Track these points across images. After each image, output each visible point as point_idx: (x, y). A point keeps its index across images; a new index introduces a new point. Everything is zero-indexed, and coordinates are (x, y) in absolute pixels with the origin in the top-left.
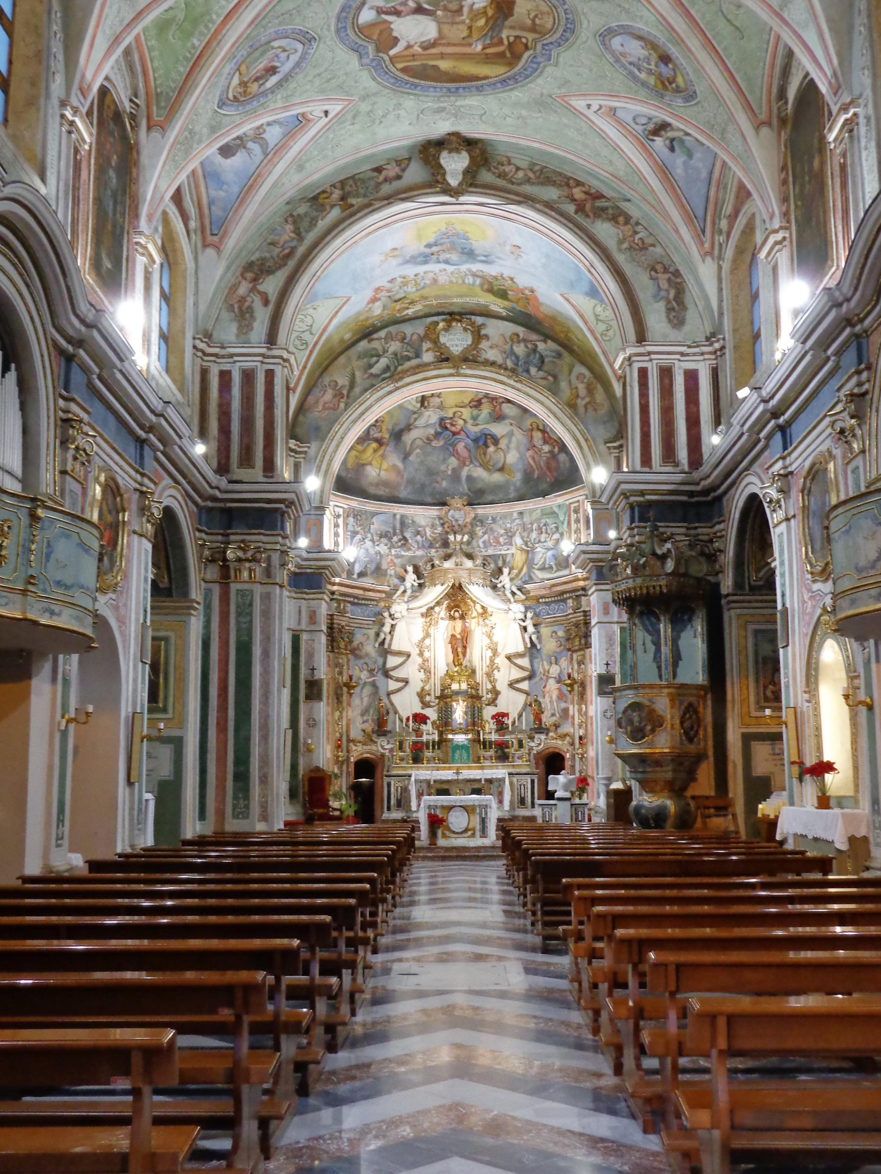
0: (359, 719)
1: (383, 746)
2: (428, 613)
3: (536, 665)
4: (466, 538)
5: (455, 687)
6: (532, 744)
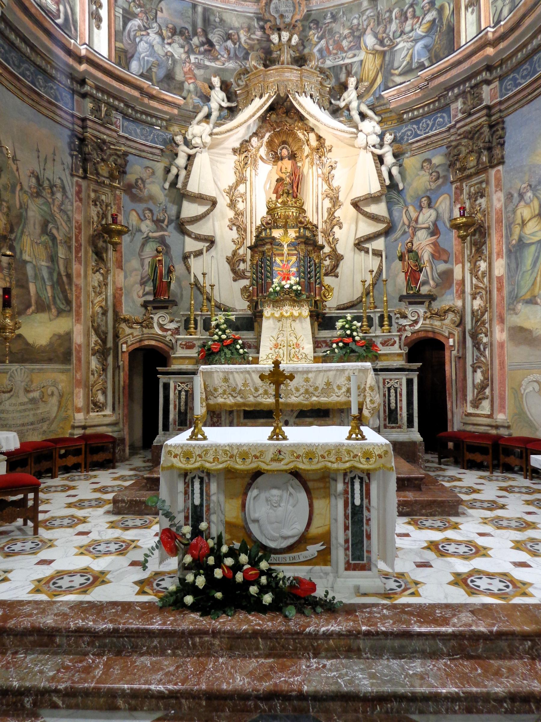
1: (163, 325)
2: (243, 148)
3: (396, 214)
4: (295, 39)
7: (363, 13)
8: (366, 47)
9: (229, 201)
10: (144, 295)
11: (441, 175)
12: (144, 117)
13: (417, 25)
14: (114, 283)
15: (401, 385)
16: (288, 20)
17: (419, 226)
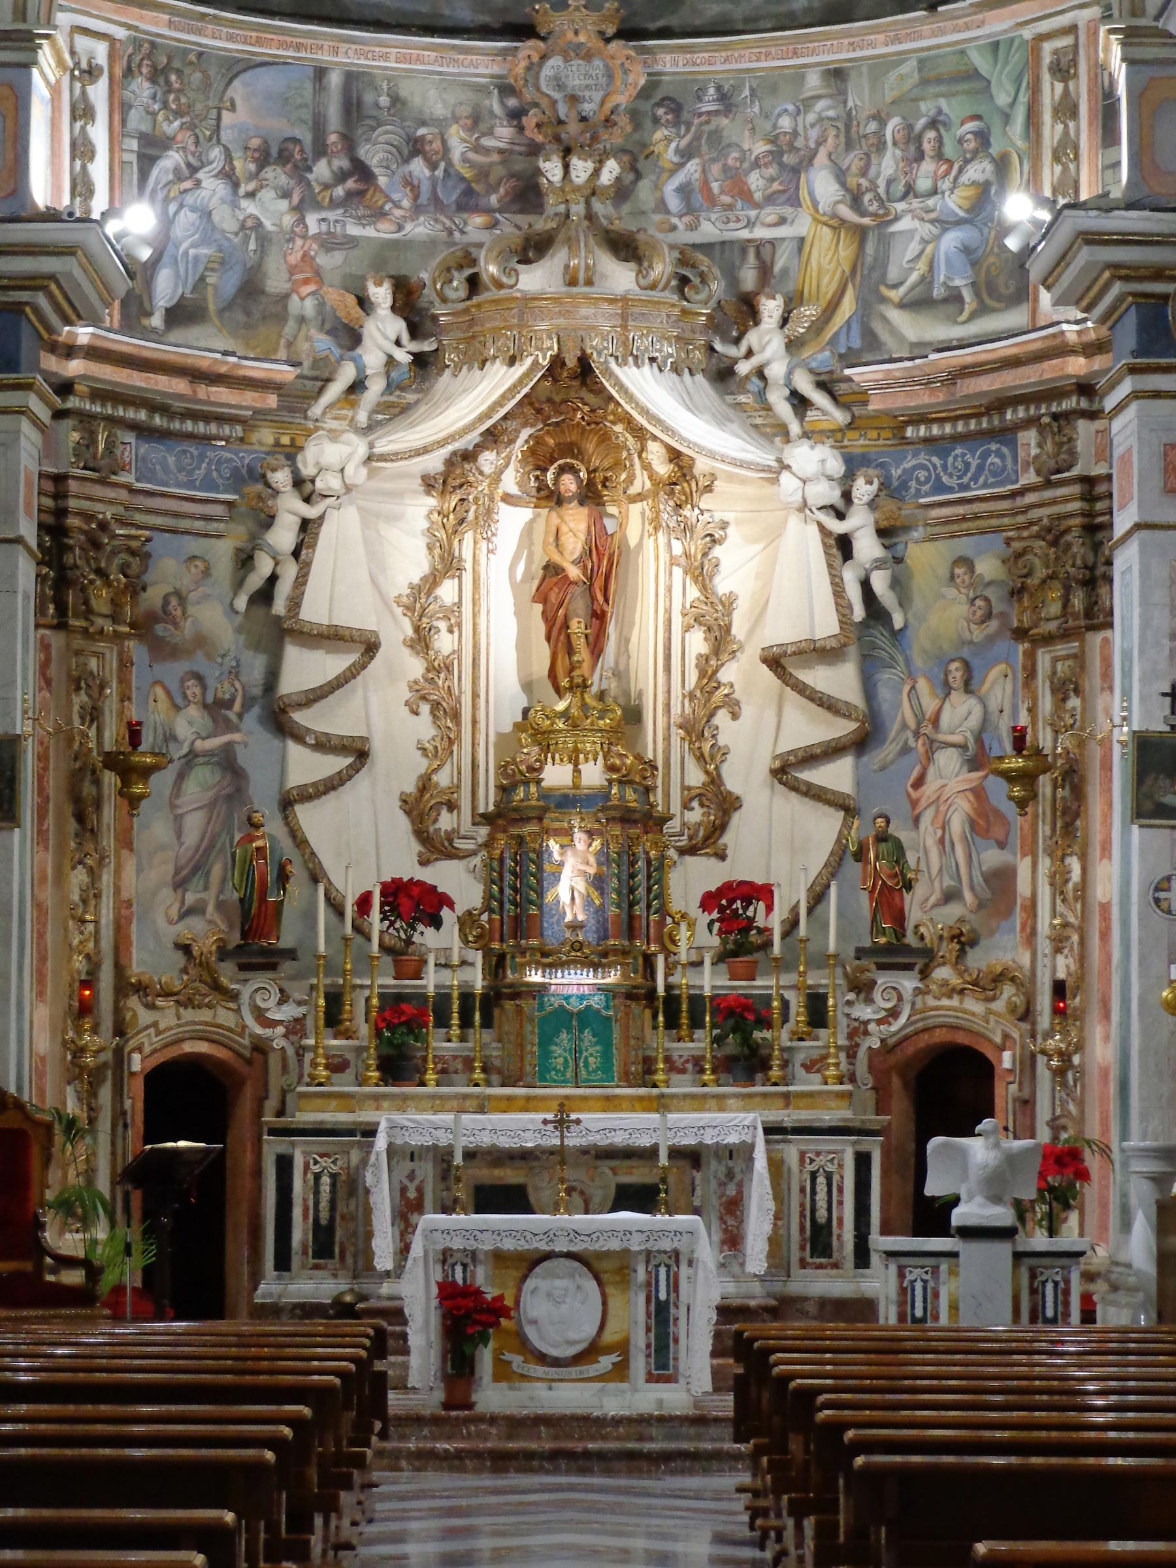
0: (167, 902)
1: (266, 1009)
2: (453, 475)
3: (884, 694)
4: (611, 170)
5: (556, 775)
6: (864, 1012)
7: (808, 103)
8: (815, 204)
9: (410, 632)
10: (183, 916)
11: (997, 607)
12: (189, 426)
13: (946, 185)
14: (117, 890)
15: (841, 1166)
16: (587, 108)
17: (942, 737)
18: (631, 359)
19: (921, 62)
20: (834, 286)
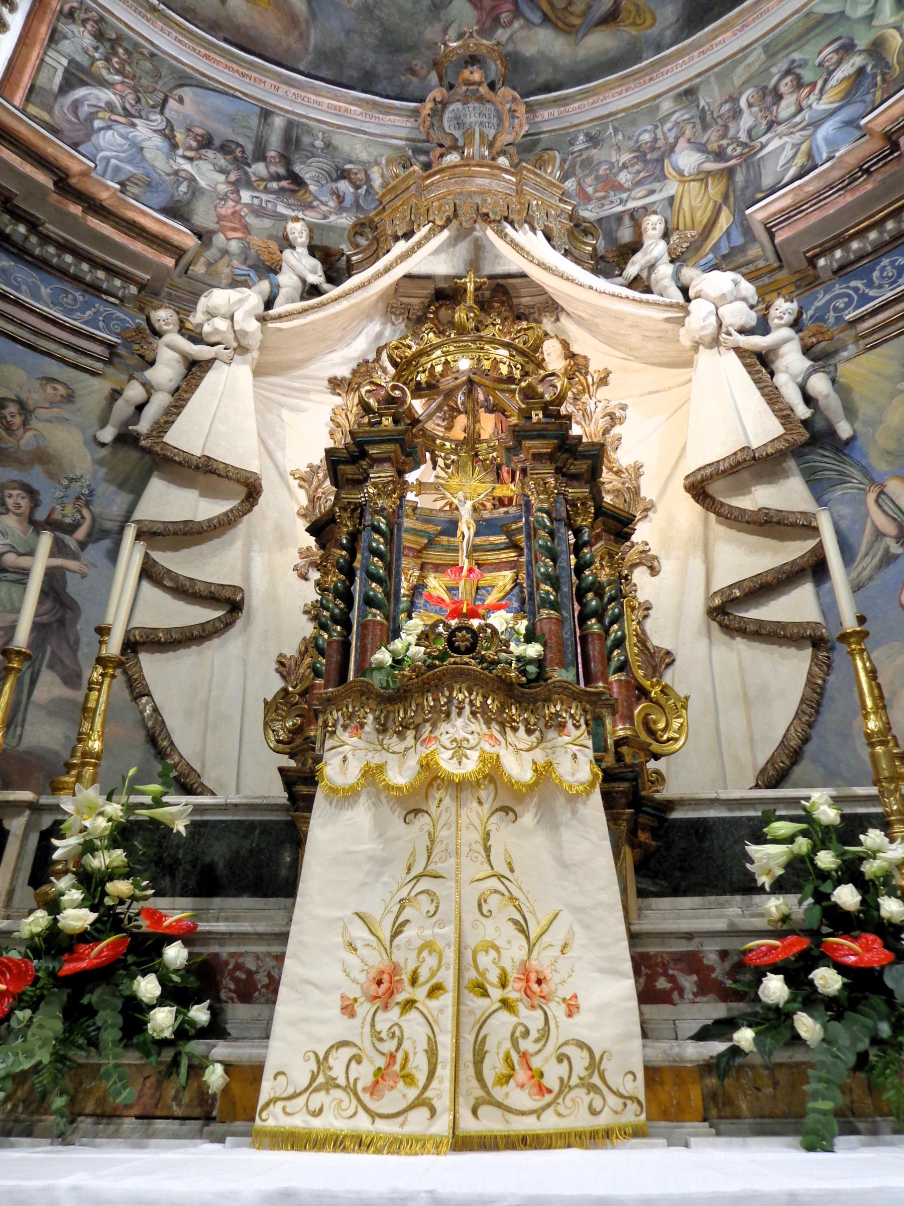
9: (305, 502)
18: (526, 226)
19: (766, 48)
20: (708, 214)
